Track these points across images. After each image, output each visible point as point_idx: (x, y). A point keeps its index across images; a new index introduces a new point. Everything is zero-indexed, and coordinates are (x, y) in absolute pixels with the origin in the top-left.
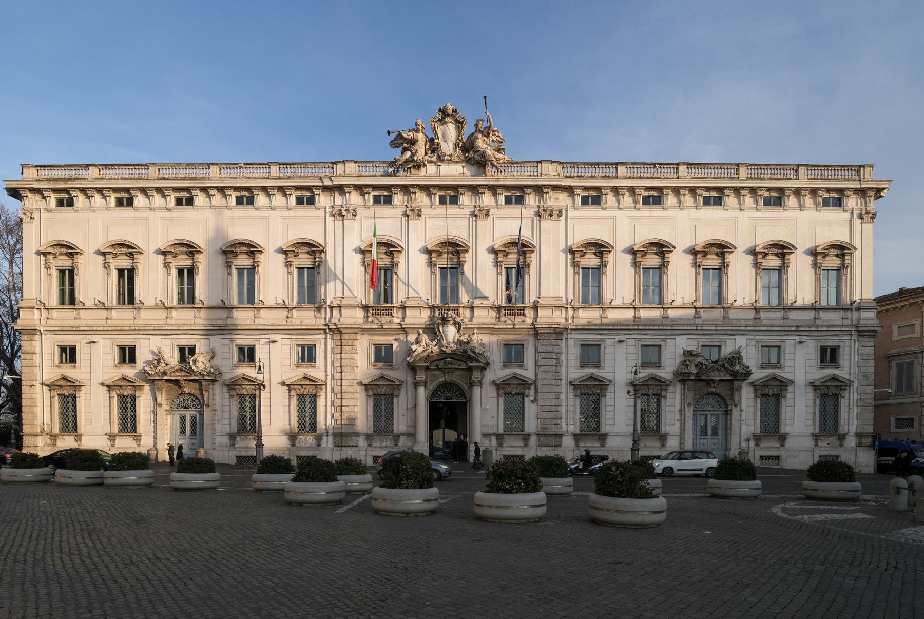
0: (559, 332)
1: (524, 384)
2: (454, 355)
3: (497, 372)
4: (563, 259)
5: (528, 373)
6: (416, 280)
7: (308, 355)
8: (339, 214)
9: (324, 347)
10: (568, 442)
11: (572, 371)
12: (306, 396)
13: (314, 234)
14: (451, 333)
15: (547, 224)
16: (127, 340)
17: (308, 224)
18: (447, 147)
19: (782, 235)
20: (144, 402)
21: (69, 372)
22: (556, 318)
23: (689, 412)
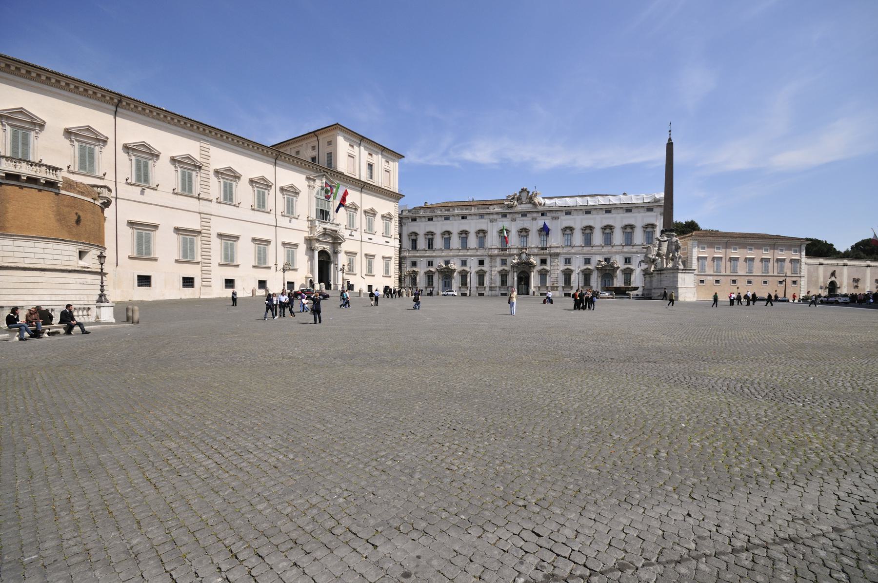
0: (558, 255)
1: (547, 271)
2: (525, 263)
3: (539, 267)
4: (560, 233)
5: (547, 268)
6: (514, 241)
7: (481, 263)
8: (491, 221)
9: (487, 261)
10: (560, 289)
11: (562, 267)
12: (481, 275)
13: (484, 227)
14: (524, 256)
15: (554, 221)
16: (430, 259)
17: (483, 224)
18: (524, 199)
19: (631, 222)
20: (436, 278)
21: (415, 269)
22: (558, 251)
23: (600, 279)
